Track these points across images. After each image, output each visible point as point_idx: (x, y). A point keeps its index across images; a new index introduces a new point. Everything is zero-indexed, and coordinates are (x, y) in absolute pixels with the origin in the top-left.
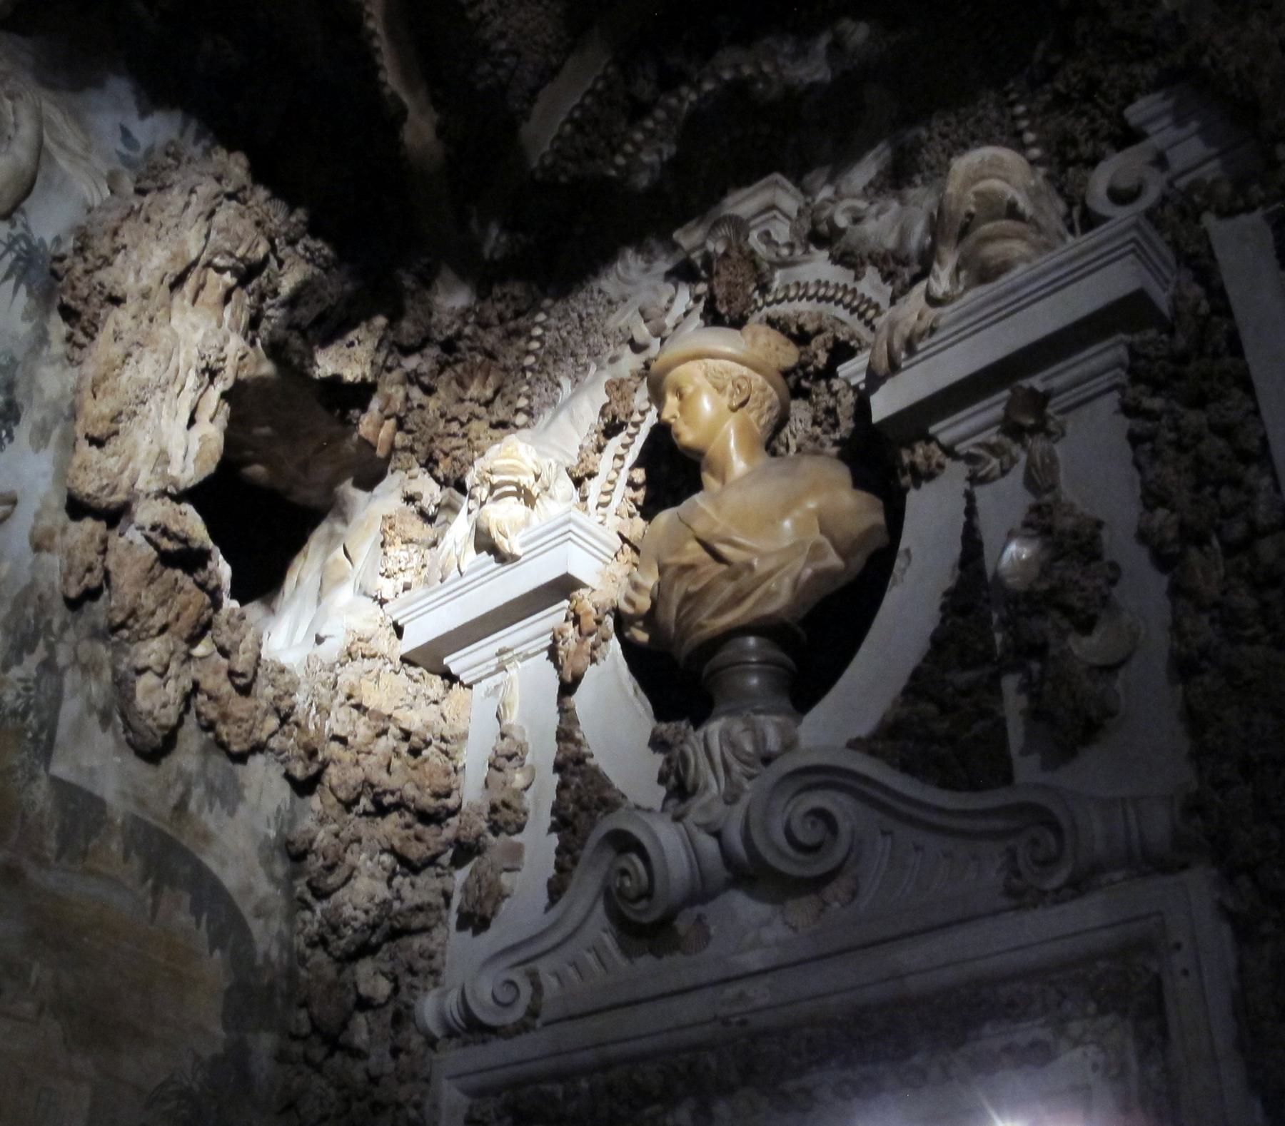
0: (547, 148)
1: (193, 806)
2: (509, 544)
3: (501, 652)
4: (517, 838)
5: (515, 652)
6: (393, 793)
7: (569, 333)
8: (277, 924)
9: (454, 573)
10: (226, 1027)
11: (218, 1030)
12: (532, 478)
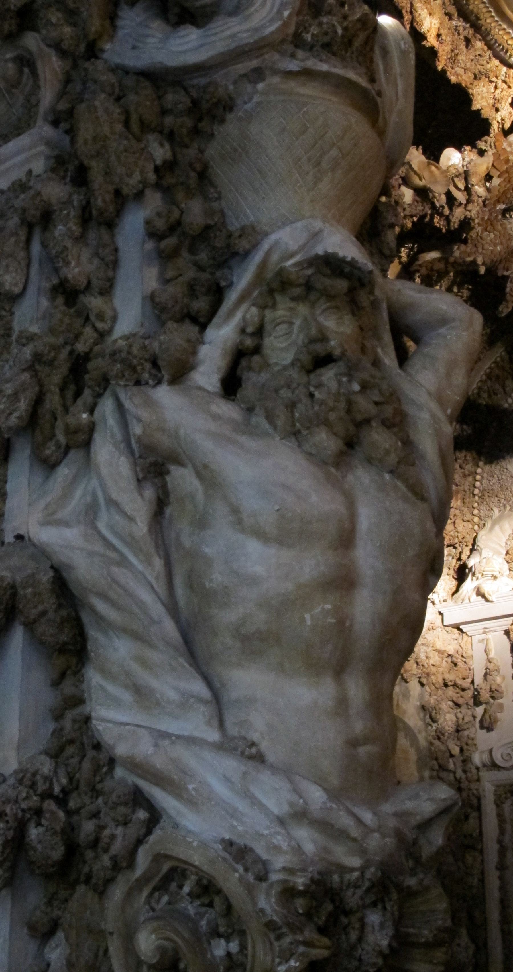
0: (475, 386)
1: (400, 703)
2: (490, 598)
3: (485, 628)
4: (500, 701)
5: (491, 629)
6: (451, 681)
7: (494, 484)
8: (424, 734)
9: (467, 601)
10: (418, 772)
11: (416, 774)
12: (498, 573)
